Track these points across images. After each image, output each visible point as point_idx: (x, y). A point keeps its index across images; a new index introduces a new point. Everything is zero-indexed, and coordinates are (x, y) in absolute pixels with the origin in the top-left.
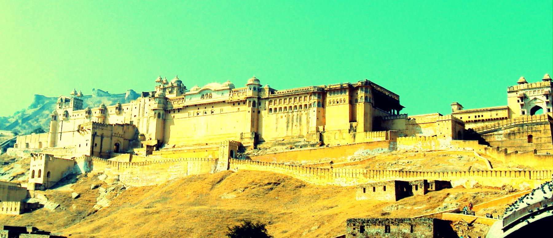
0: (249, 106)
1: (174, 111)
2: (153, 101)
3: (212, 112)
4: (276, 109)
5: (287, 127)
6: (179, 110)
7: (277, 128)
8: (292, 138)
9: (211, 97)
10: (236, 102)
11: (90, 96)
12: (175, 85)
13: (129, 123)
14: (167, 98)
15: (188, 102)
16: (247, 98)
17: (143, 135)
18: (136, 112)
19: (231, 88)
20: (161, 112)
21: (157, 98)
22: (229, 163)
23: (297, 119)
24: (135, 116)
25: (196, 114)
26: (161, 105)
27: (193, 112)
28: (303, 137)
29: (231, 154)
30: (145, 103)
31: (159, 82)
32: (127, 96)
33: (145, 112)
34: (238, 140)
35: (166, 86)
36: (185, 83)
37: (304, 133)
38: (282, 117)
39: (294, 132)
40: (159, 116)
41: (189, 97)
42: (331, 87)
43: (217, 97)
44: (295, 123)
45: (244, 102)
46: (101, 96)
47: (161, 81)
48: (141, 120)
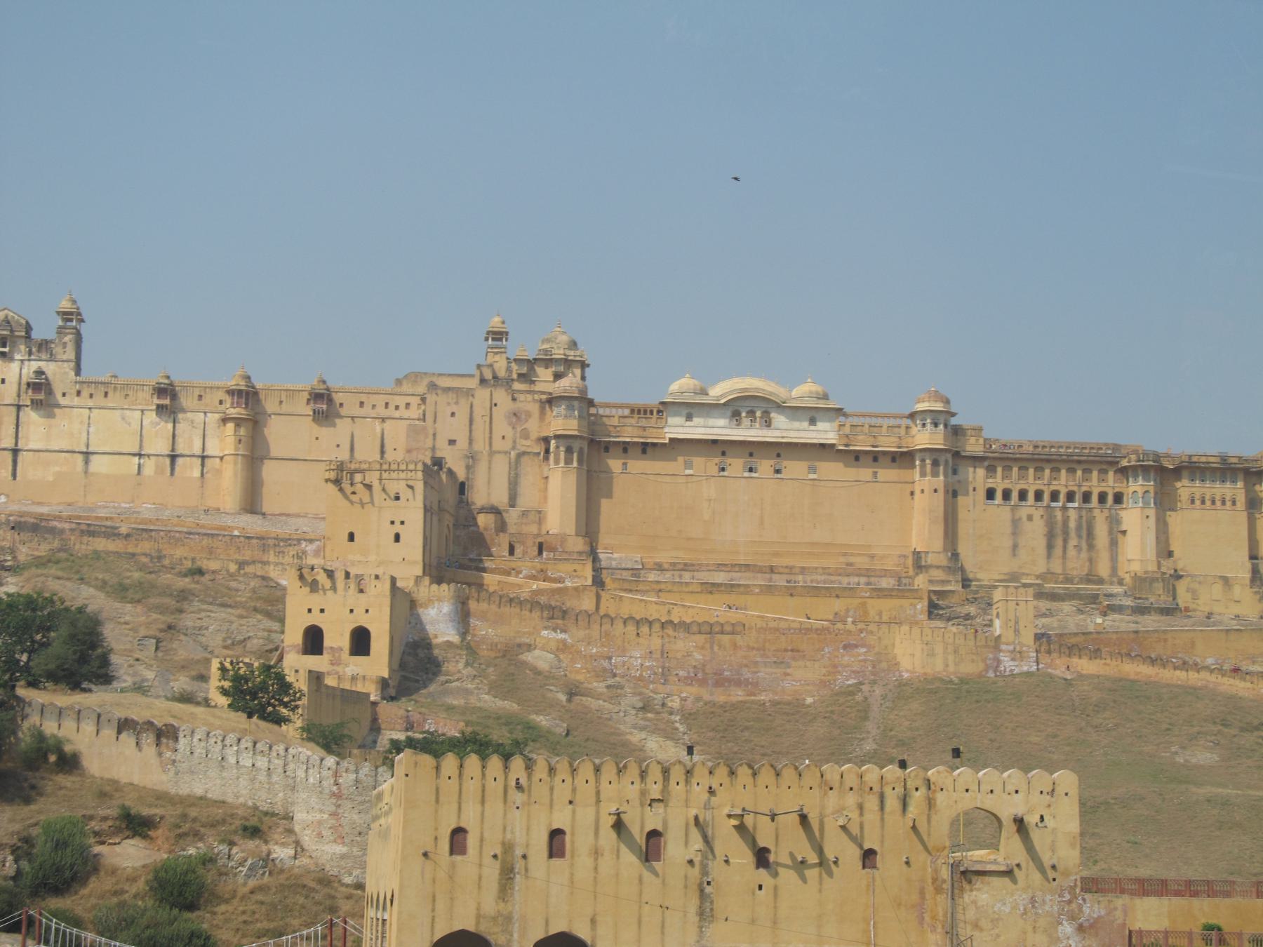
4: (1007, 495)
5: (1050, 547)
6: (646, 449)
7: (1015, 547)
8: (1068, 580)
9: (768, 424)
17: (495, 511)
23: (1079, 528)
24: (452, 442)
25: (714, 470)
28: (1101, 581)
37: (1103, 570)
38: (1030, 518)
39: (1070, 565)
40: (580, 461)
41: (685, 412)
42: (1194, 459)
44: (1073, 542)
45: (903, 458)
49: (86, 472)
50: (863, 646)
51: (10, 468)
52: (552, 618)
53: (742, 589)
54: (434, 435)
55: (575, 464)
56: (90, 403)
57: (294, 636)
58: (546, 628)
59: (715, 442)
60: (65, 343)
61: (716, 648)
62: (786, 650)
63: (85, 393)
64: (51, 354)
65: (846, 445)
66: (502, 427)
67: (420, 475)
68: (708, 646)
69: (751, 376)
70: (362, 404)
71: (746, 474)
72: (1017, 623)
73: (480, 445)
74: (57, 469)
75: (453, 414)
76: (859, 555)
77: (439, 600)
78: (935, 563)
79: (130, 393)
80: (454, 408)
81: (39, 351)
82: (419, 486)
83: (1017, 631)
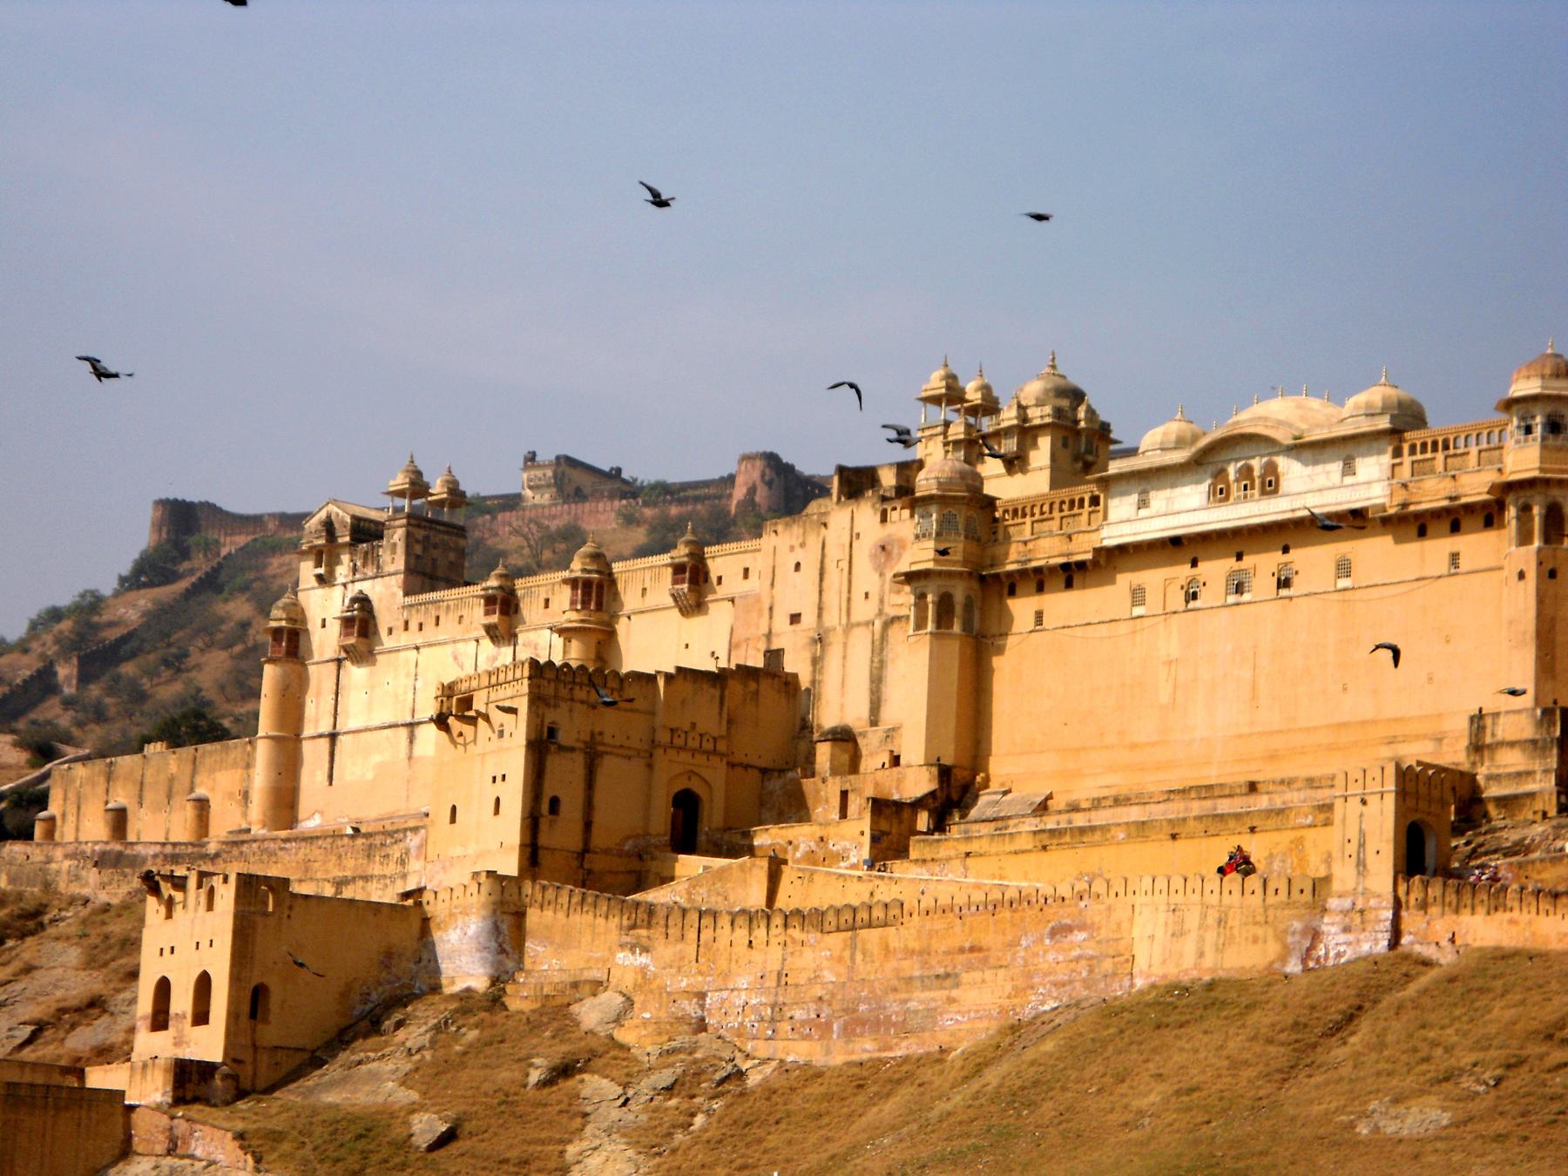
0: (1524, 538)
1: (1039, 579)
2: (903, 523)
3: (1284, 583)
6: (1071, 574)
9: (1271, 485)
10: (1437, 514)
11: (512, 502)
12: (1038, 415)
13: (758, 662)
14: (990, 502)
15: (1125, 520)
16: (1510, 487)
17: (844, 737)
18: (797, 593)
19: (1403, 426)
20: (959, 594)
21: (928, 500)
22: (1398, 905)
24: (795, 618)
26: (958, 547)
27: (1162, 580)
29: (1415, 855)
30: (854, 536)
31: (935, 400)
32: (739, 493)
33: (858, 596)
34: (1455, 755)
35: (987, 424)
36: (1104, 403)
43: (1309, 488)
45: (1488, 515)
46: (579, 495)
47: (952, 395)
48: (836, 640)
49: (410, 758)
50: (1082, 927)
51: (327, 766)
52: (634, 927)
53: (1097, 836)
54: (771, 609)
55: (957, 628)
56: (419, 641)
57: (145, 1005)
58: (622, 946)
59: (1176, 541)
60: (395, 545)
61: (859, 957)
62: (962, 950)
63: (413, 626)
64: (378, 567)
65: (1405, 505)
66: (867, 578)
67: (526, 682)
68: (847, 954)
69: (1351, 395)
70: (746, 570)
71: (1232, 599)
72: (1362, 845)
73: (832, 618)
74: (377, 758)
75: (798, 566)
76: (1418, 737)
77: (465, 913)
78: (1510, 737)
79: (464, 612)
80: (799, 555)
81: (364, 565)
82: (523, 705)
83: (1361, 864)
